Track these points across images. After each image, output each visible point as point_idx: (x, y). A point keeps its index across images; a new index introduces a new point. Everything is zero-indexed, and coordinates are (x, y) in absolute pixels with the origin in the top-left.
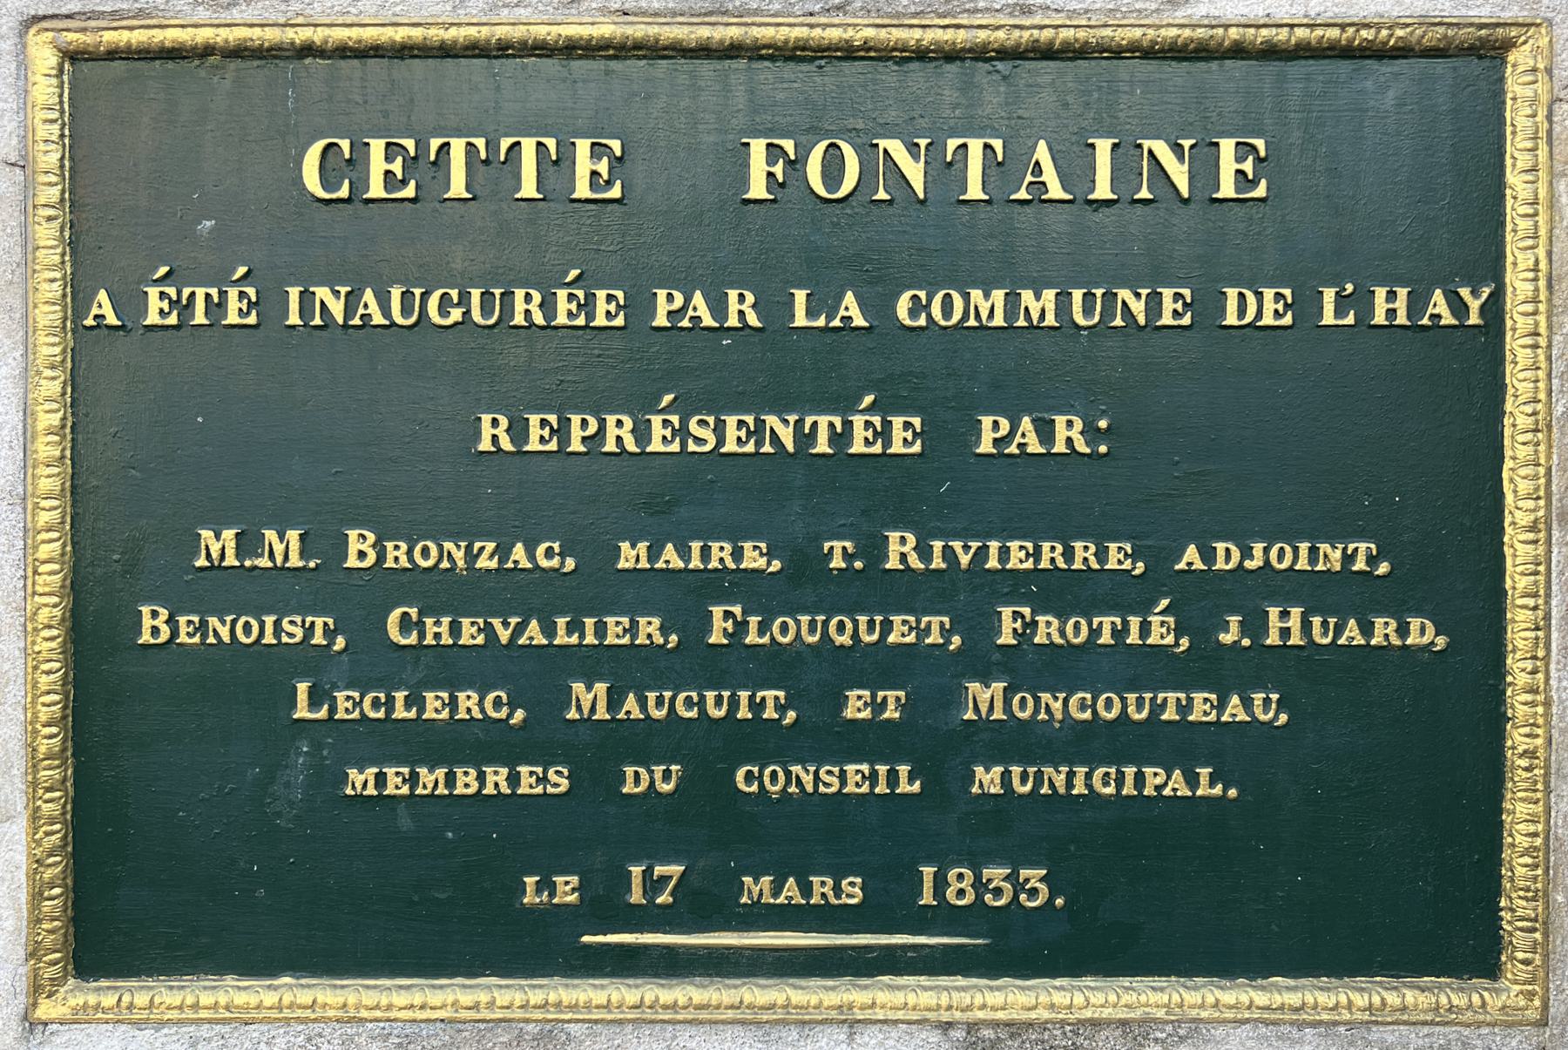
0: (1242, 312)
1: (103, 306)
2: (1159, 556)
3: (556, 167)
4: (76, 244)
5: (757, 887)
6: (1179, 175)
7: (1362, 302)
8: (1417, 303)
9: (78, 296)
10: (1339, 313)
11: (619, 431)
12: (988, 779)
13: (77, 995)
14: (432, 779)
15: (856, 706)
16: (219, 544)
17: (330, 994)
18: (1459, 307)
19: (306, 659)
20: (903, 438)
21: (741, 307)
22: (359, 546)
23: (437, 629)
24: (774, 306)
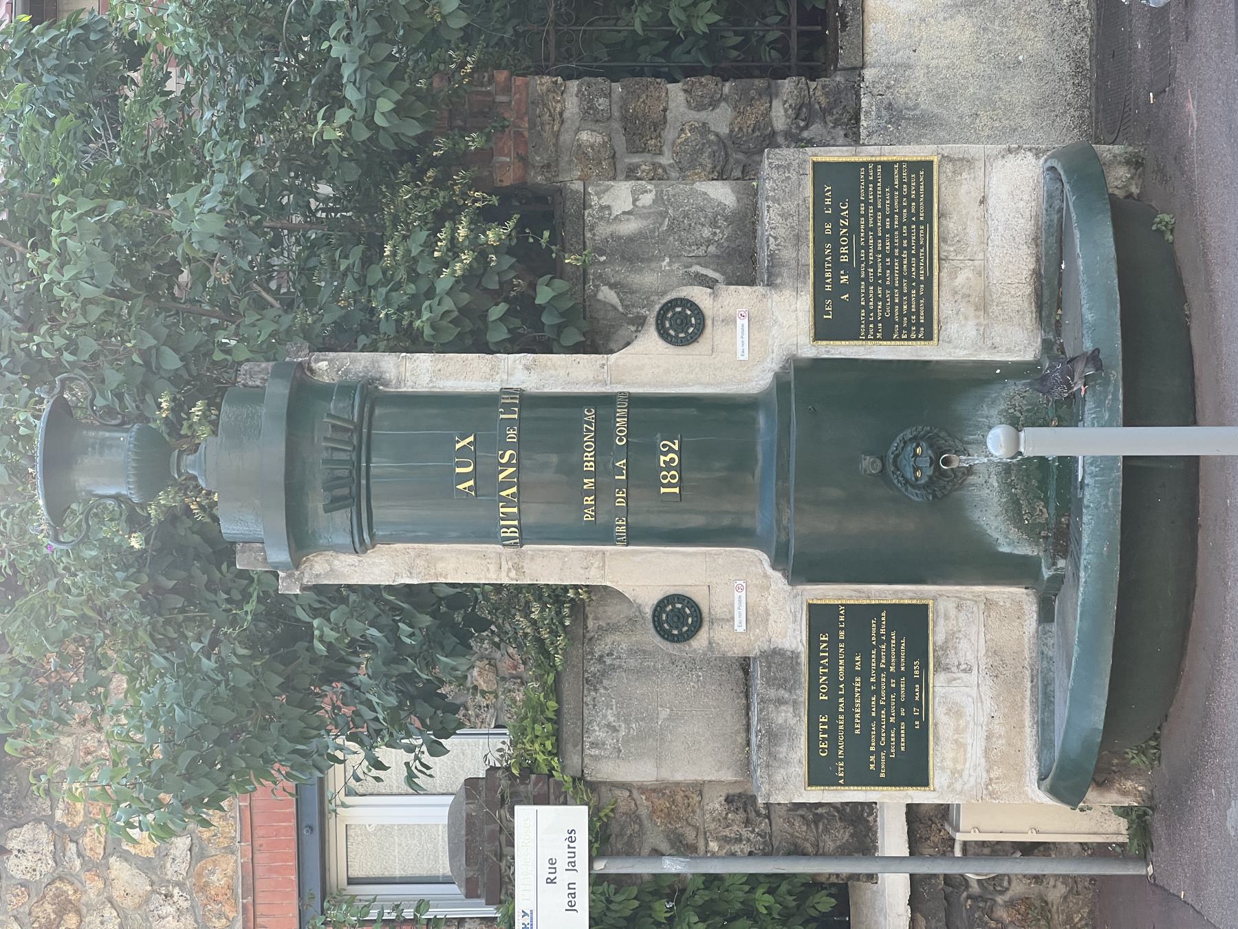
1: (841, 781)
2: (873, 647)
3: (824, 723)
4: (833, 785)
5: (917, 698)
6: (825, 645)
9: (841, 785)
11: (857, 716)
12: (903, 669)
14: (903, 740)
15: (893, 686)
16: (872, 767)
17: (931, 752)
19: (887, 756)
20: (858, 679)
21: (841, 700)
22: (872, 749)
23: (883, 739)
24: (841, 696)
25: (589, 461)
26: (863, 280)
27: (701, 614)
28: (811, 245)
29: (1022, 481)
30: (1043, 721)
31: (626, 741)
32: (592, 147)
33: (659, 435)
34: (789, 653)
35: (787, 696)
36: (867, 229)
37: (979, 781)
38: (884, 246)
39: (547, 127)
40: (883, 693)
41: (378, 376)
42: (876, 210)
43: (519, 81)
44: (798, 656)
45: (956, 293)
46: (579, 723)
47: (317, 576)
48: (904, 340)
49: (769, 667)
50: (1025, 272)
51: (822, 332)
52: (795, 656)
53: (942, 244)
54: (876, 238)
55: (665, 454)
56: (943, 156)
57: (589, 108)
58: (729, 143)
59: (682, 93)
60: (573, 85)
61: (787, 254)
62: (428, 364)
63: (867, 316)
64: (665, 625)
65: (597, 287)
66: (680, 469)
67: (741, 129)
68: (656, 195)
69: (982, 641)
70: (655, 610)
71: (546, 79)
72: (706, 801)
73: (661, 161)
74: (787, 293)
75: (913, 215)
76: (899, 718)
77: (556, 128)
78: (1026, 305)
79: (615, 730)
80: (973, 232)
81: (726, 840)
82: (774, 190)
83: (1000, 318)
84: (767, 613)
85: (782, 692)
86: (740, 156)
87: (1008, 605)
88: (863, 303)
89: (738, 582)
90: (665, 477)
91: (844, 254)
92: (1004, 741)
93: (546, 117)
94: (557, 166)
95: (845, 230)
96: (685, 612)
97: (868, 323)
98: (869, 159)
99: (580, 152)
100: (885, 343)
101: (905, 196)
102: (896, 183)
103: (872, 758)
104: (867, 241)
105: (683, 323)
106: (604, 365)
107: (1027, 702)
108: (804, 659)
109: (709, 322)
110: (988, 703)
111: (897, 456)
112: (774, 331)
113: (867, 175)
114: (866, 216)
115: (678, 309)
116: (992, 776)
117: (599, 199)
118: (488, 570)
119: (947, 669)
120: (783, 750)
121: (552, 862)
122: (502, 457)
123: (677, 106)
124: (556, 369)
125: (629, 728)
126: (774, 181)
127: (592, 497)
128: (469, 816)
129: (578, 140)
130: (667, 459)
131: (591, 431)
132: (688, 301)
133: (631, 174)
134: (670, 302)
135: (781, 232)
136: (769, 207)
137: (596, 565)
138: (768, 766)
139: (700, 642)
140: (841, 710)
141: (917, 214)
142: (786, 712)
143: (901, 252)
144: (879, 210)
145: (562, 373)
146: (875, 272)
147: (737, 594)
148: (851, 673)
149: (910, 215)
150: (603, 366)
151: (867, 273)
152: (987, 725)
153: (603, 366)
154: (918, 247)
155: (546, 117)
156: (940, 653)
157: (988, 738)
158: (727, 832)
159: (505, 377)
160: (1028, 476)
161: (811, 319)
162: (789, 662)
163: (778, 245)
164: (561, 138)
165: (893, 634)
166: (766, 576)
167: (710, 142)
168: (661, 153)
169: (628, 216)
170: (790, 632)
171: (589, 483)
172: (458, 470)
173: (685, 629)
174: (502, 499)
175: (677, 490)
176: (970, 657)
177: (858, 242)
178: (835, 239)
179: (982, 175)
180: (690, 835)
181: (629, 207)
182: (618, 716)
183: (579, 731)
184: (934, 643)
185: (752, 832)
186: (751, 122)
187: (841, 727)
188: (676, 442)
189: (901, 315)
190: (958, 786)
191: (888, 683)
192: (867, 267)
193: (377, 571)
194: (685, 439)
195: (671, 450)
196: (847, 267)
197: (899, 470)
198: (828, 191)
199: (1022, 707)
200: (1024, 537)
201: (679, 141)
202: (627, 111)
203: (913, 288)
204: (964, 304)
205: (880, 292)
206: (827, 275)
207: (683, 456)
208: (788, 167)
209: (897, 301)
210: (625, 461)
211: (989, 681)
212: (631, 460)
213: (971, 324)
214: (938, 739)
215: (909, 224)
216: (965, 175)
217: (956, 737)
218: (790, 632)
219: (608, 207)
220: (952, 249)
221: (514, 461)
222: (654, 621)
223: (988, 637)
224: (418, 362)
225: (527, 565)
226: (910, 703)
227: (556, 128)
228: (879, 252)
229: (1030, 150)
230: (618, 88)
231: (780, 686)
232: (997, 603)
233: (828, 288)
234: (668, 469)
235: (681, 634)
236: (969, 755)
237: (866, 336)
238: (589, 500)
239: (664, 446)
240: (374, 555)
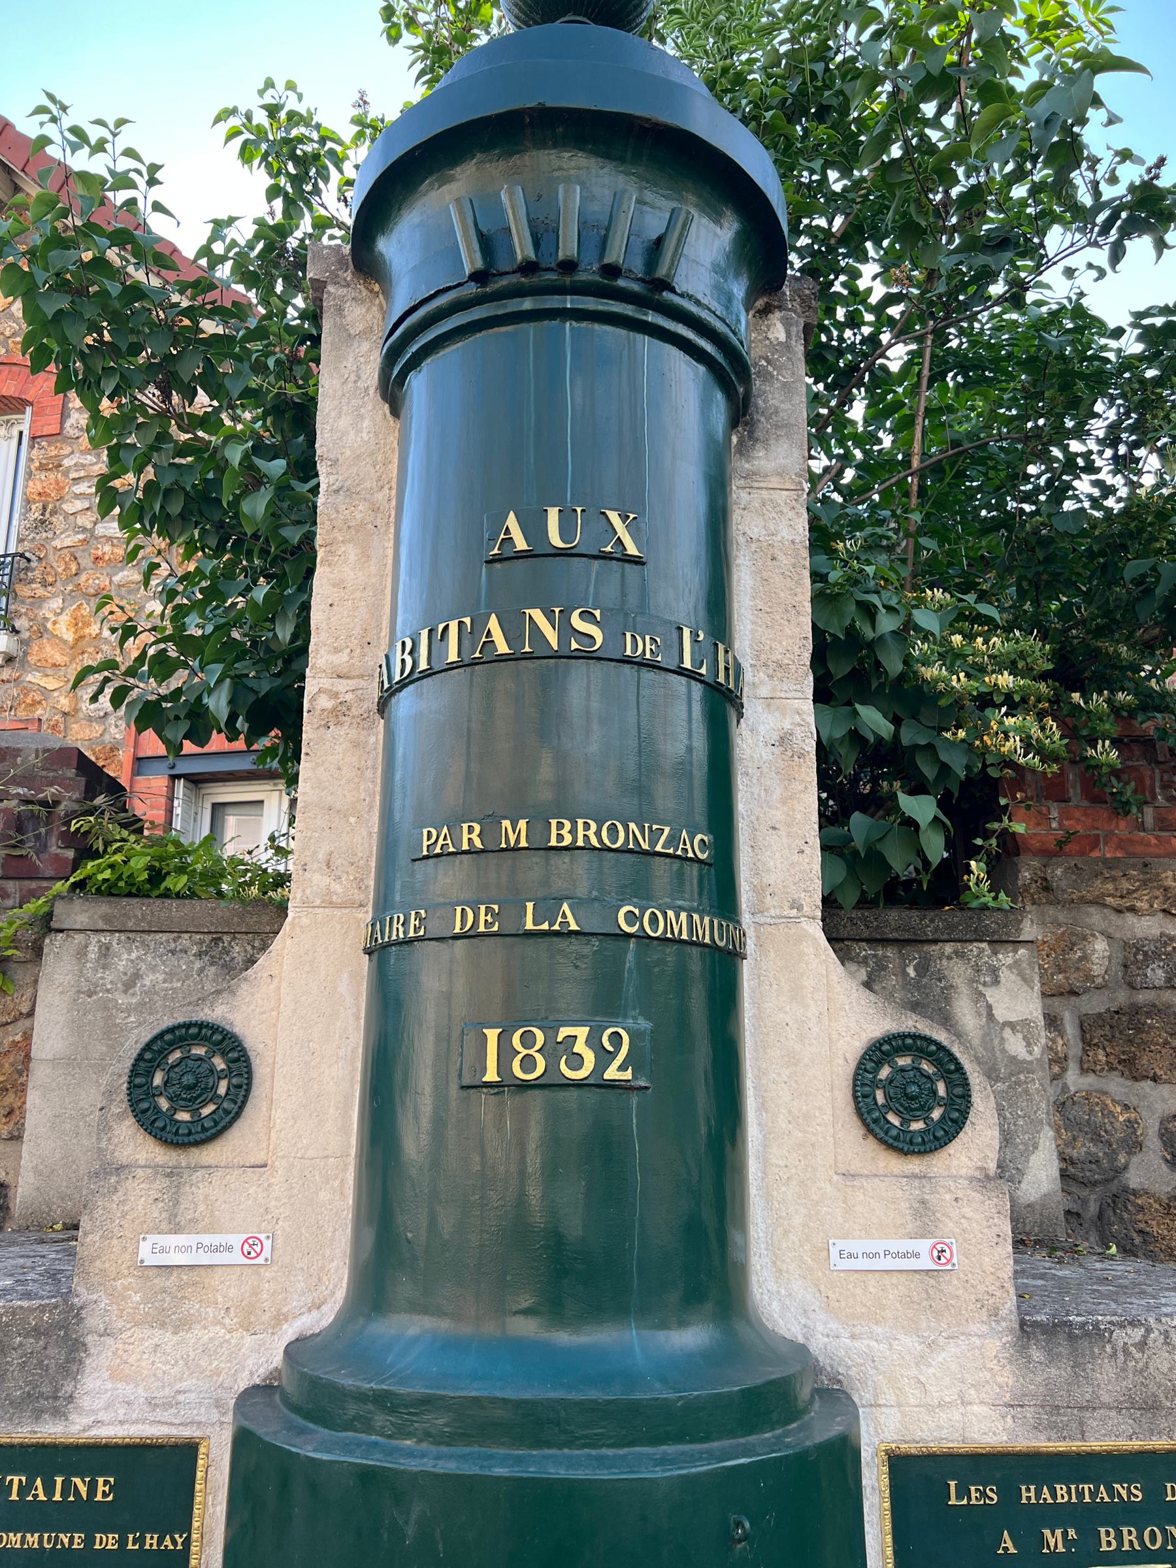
0: (101, 1544)
6: (83, 1490)
7: (141, 1540)
8: (160, 1541)
10: (134, 1544)
18: (174, 1542)
25: (574, 831)
27: (197, 1144)
28: (1136, 1444)
31: (105, 1006)
32: (1085, 958)
33: (644, 1024)
34: (69, 1388)
39: (1110, 886)
41: (759, 434)
44: (59, 1413)
46: (144, 926)
47: (340, 310)
49: (37, 1332)
55: (593, 1041)
57: (1145, 954)
58: (1114, 1187)
62: (785, 533)
64: (177, 1055)
65: (864, 962)
66: (551, 1084)
67: (1141, 1209)
68: (1024, 1061)
73: (1070, 1072)
74: (1006, 1378)
77: (1109, 900)
79: (129, 986)
84: (183, 1324)
86: (1093, 1208)
89: (267, 1244)
90: (528, 1039)
91: (1119, 1537)
93: (1126, 885)
94: (1050, 903)
96: (185, 1109)
99: (1073, 940)
106: (800, 908)
108: (51, 1431)
109: (914, 1165)
112: (908, 1343)
117: (1010, 967)
118: (337, 650)
122: (587, 616)
123: (1164, 1100)
124: (784, 801)
125: (129, 1010)
127: (478, 844)
128: (17, 752)
129: (1094, 935)
130: (580, 1047)
131: (653, 843)
132: (964, 1114)
133: (1052, 1022)
134: (959, 1068)
137: (337, 887)
147: (236, 1240)
150: (796, 905)
155: (1126, 885)
159: (764, 691)
162: (46, 1389)
163: (1126, 1352)
164: (1092, 910)
166: (280, 1319)
167: (1112, 1156)
168: (1084, 1071)
169: (984, 1013)
171: (515, 832)
172: (553, 515)
173: (164, 1104)
174: (479, 623)
175: (491, 1076)
181: (1000, 1014)
182: (152, 991)
183: (130, 924)
188: (628, 1075)
193: (344, 422)
194: (634, 1100)
195: (604, 1058)
201: (1109, 1102)
202: (1148, 1015)
206: (1062, 1490)
207: (585, 1093)
210: (574, 927)
212: (575, 945)
218: (126, 1389)
219: (996, 982)
221: (574, 645)
222: (188, 1026)
224: (791, 514)
225: (343, 733)
227: (1109, 900)
233: (1028, 1494)
234: (553, 1050)
238: (471, 836)
239: (616, 1038)
240: (379, 417)
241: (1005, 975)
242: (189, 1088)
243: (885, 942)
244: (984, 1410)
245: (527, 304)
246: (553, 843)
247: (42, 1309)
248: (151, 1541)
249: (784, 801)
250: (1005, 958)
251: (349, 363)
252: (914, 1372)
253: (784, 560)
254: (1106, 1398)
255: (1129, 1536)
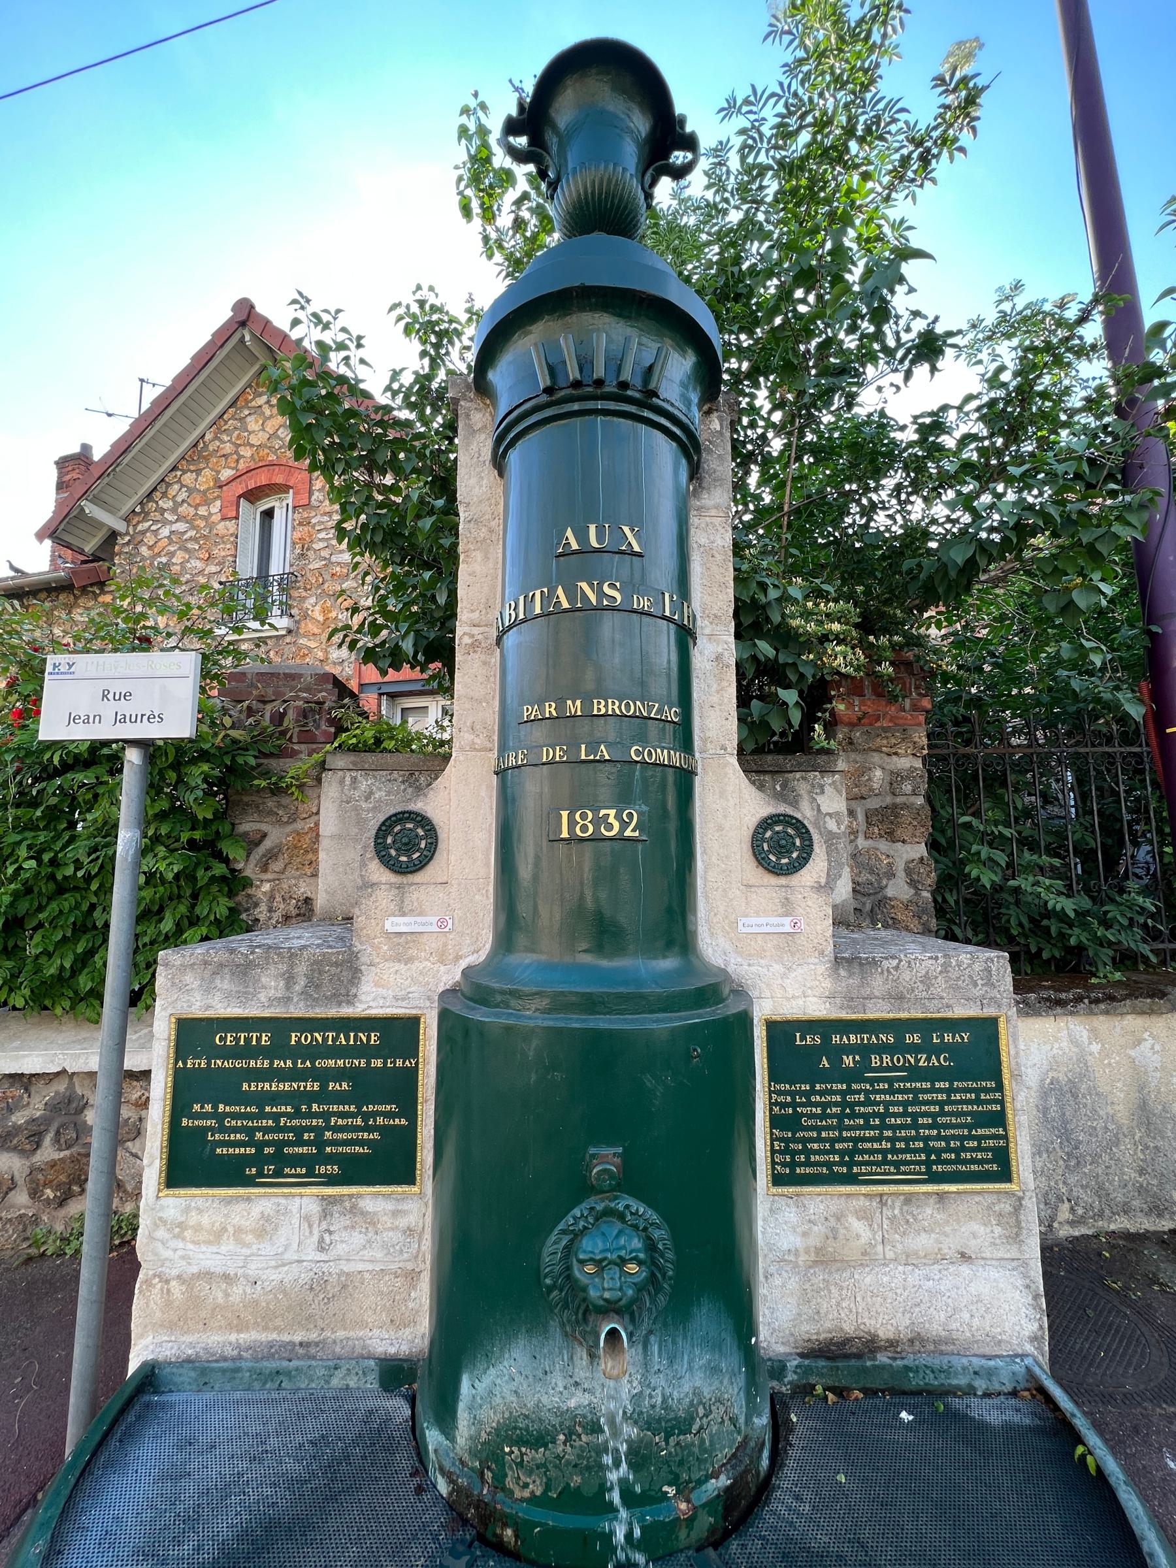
1: (180, 1064)
2: (359, 1108)
3: (259, 1039)
5: (287, 1170)
6: (364, 1039)
7: (395, 1062)
9: (176, 1062)
11: (267, 1086)
12: (328, 1149)
13: (166, 1192)
14: (231, 1151)
15: (306, 1136)
19: (211, 1128)
20: (316, 1088)
21: (289, 1063)
25: (606, 706)
26: (849, 1086)
27: (411, 872)
28: (891, 1016)
29: (579, 1457)
30: (238, 1370)
31: (356, 809)
32: (870, 779)
33: (645, 808)
34: (354, 991)
35: (297, 988)
36: (916, 1092)
37: (167, 1264)
38: (895, 1115)
39: (885, 742)
40: (295, 1122)
41: (705, 485)
42: (941, 1104)
43: (922, 718)
44: (350, 1003)
45: (838, 1219)
46: (373, 767)
47: (468, 416)
48: (772, 1145)
49: (336, 964)
50: (873, 1322)
51: (780, 1031)
52: (350, 1000)
53: (902, 1198)
54: (905, 1104)
55: (618, 817)
56: (1020, 1199)
58: (879, 896)
59: (919, 856)
60: (918, 764)
61: (877, 984)
62: (719, 542)
63: (802, 1093)
64: (399, 828)
66: (596, 839)
69: (361, 1267)
70: (417, 814)
71: (925, 741)
72: (308, 880)
74: (827, 984)
75: (938, 1156)
76: (260, 1146)
77: (884, 749)
78: (828, 1325)
79: (367, 798)
80: (923, 1242)
81: (272, 898)
82: (959, 966)
83: (807, 1286)
84: (409, 960)
85: (302, 981)
86: (868, 907)
87: (411, 1305)
88: (818, 1087)
89: (450, 922)
90: (584, 817)
91: (881, 1060)
92: (220, 1301)
93: (893, 741)
94: (853, 751)
95: (912, 1061)
96: (404, 855)
97: (792, 1094)
98: (1007, 1093)
99: (864, 770)
100: (768, 1119)
101: (962, 1144)
102: (980, 1132)
103: (208, 1108)
104: (900, 1091)
105: (781, 848)
106: (725, 749)
107: (274, 1336)
108: (346, 1011)
109: (783, 881)
110: (275, 1276)
111: (621, 1217)
112: (777, 968)
113: (987, 1090)
114: (933, 1090)
115: (798, 842)
116: (173, 1283)
118: (472, 611)
119: (325, 1214)
120: (225, 983)
121: (126, 696)
122: (612, 586)
124: (718, 692)
125: (368, 811)
126: (969, 966)
127: (554, 714)
128: (300, 676)
130: (611, 820)
131: (650, 712)
132: (809, 855)
133: (851, 813)
134: (808, 831)
135: (906, 976)
136: (937, 958)
137: (477, 741)
138: (206, 963)
139: (378, 873)
140: (276, 1062)
141: (940, 1161)
142: (276, 989)
143: (888, 1139)
144: (942, 1108)
145: (715, 699)
146: (860, 1104)
147: (434, 919)
148: (324, 1076)
149: (939, 1152)
150: (724, 748)
151: (858, 1092)
152: (246, 1276)
153: (724, 748)
154: (897, 1164)
155: (893, 741)
156: (347, 1204)
157: (226, 1277)
158: (278, 899)
159: (707, 631)
160: (588, 1468)
161: (795, 1017)
162: (343, 991)
163: (888, 971)
164: (874, 754)
165: (376, 1136)
166: (458, 958)
167: (879, 881)
168: (866, 838)
170: (383, 992)
171: (575, 707)
172: (592, 529)
173: (393, 852)
174: (552, 591)
175: (565, 835)
176: (341, 1249)
177: (900, 1079)
178: (899, 1048)
179: (1000, 1255)
180: (276, 866)
181: (824, 809)
182: (380, 800)
183: (366, 766)
184: (360, 1196)
185: (278, 922)
186: (899, 917)
187: (252, 1063)
188: (637, 834)
189: (804, 1141)
190: (161, 1233)
191: (310, 1129)
192: (867, 1092)
193: (473, 481)
194: (640, 846)
195: (624, 825)
196: (866, 1065)
197: (597, 1219)
198: (962, 1038)
199: (265, 1328)
200: (484, 1436)
202: (902, 809)
203: (842, 1157)
204: (823, 1230)
205: (834, 1109)
207: (613, 843)
208: (989, 983)
209: (824, 1134)
210: (607, 757)
211: (305, 1277)
212: (608, 767)
213: (797, 1242)
214: (229, 1203)
215: (927, 1150)
216: (998, 1230)
217: (231, 1229)
218: (383, 992)
219: (823, 792)
220: (896, 1212)
221: (605, 603)
222: (403, 813)
223: (367, 1276)
224: (723, 531)
225: (477, 657)
226: (282, 1161)
227: (884, 749)
228: (887, 1109)
229: (1041, 1327)
230: (920, 801)
231: (309, 977)
232: (414, 1288)
233: (836, 1039)
234: (597, 822)
235: (387, 848)
236: (204, 1248)
237: (774, 1092)
238: (550, 709)
239: (630, 815)
240: (492, 478)
241: (827, 788)
242: (406, 844)
243: (765, 772)
244: (815, 999)
245: (576, 406)
246: (595, 712)
247: (338, 953)
248: (399, 1063)
249: (718, 692)
250: (828, 780)
251: (474, 446)
252: (780, 981)
253: (719, 557)
254: (877, 993)
255: (886, 1059)
